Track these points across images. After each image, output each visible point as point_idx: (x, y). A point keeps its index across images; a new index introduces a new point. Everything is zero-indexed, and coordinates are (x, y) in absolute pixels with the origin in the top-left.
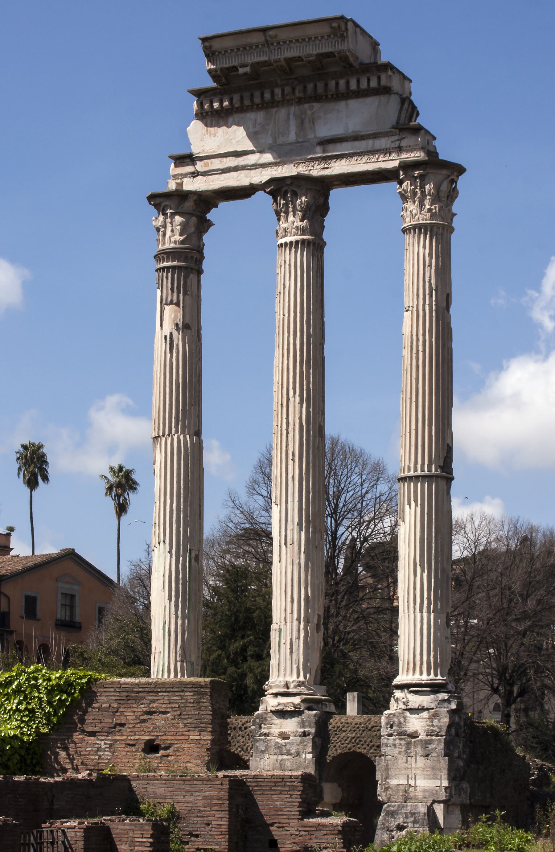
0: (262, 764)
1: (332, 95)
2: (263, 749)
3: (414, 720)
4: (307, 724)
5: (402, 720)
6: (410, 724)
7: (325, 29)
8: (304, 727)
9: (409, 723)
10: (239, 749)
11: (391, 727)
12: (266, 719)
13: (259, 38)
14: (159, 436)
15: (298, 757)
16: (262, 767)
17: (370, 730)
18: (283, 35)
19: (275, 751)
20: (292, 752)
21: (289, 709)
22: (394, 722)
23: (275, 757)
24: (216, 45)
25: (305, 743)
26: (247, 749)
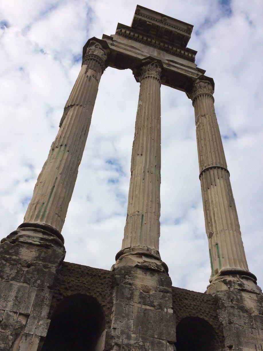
0: (127, 309)
1: (172, 53)
2: (129, 296)
3: (248, 300)
4: (165, 283)
5: (239, 297)
6: (245, 302)
7: (185, 28)
8: (163, 286)
9: (245, 301)
10: (98, 294)
11: (232, 301)
12: (130, 271)
13: (159, 18)
14: (74, 105)
15: (160, 310)
16: (127, 312)
17: (205, 302)
18: (169, 21)
19: (140, 300)
20: (156, 304)
21: (153, 268)
22: (233, 298)
23: (139, 305)
24: (142, 11)
25: (167, 299)
26: (105, 296)
